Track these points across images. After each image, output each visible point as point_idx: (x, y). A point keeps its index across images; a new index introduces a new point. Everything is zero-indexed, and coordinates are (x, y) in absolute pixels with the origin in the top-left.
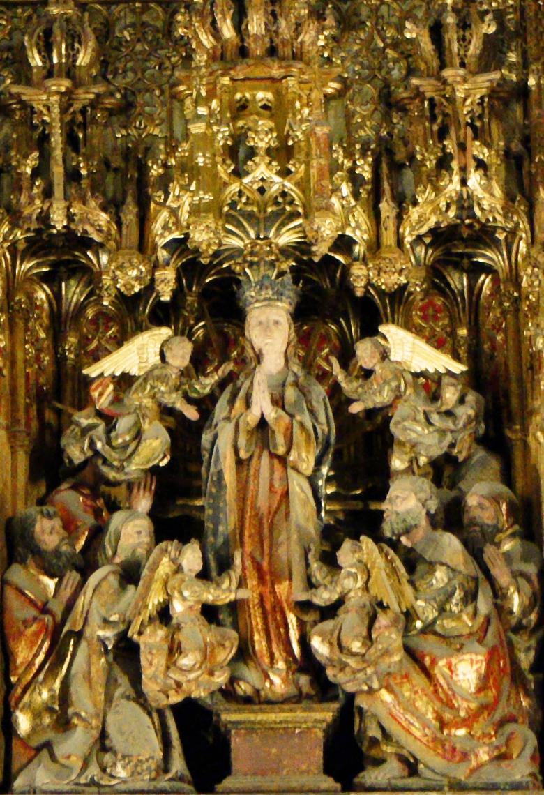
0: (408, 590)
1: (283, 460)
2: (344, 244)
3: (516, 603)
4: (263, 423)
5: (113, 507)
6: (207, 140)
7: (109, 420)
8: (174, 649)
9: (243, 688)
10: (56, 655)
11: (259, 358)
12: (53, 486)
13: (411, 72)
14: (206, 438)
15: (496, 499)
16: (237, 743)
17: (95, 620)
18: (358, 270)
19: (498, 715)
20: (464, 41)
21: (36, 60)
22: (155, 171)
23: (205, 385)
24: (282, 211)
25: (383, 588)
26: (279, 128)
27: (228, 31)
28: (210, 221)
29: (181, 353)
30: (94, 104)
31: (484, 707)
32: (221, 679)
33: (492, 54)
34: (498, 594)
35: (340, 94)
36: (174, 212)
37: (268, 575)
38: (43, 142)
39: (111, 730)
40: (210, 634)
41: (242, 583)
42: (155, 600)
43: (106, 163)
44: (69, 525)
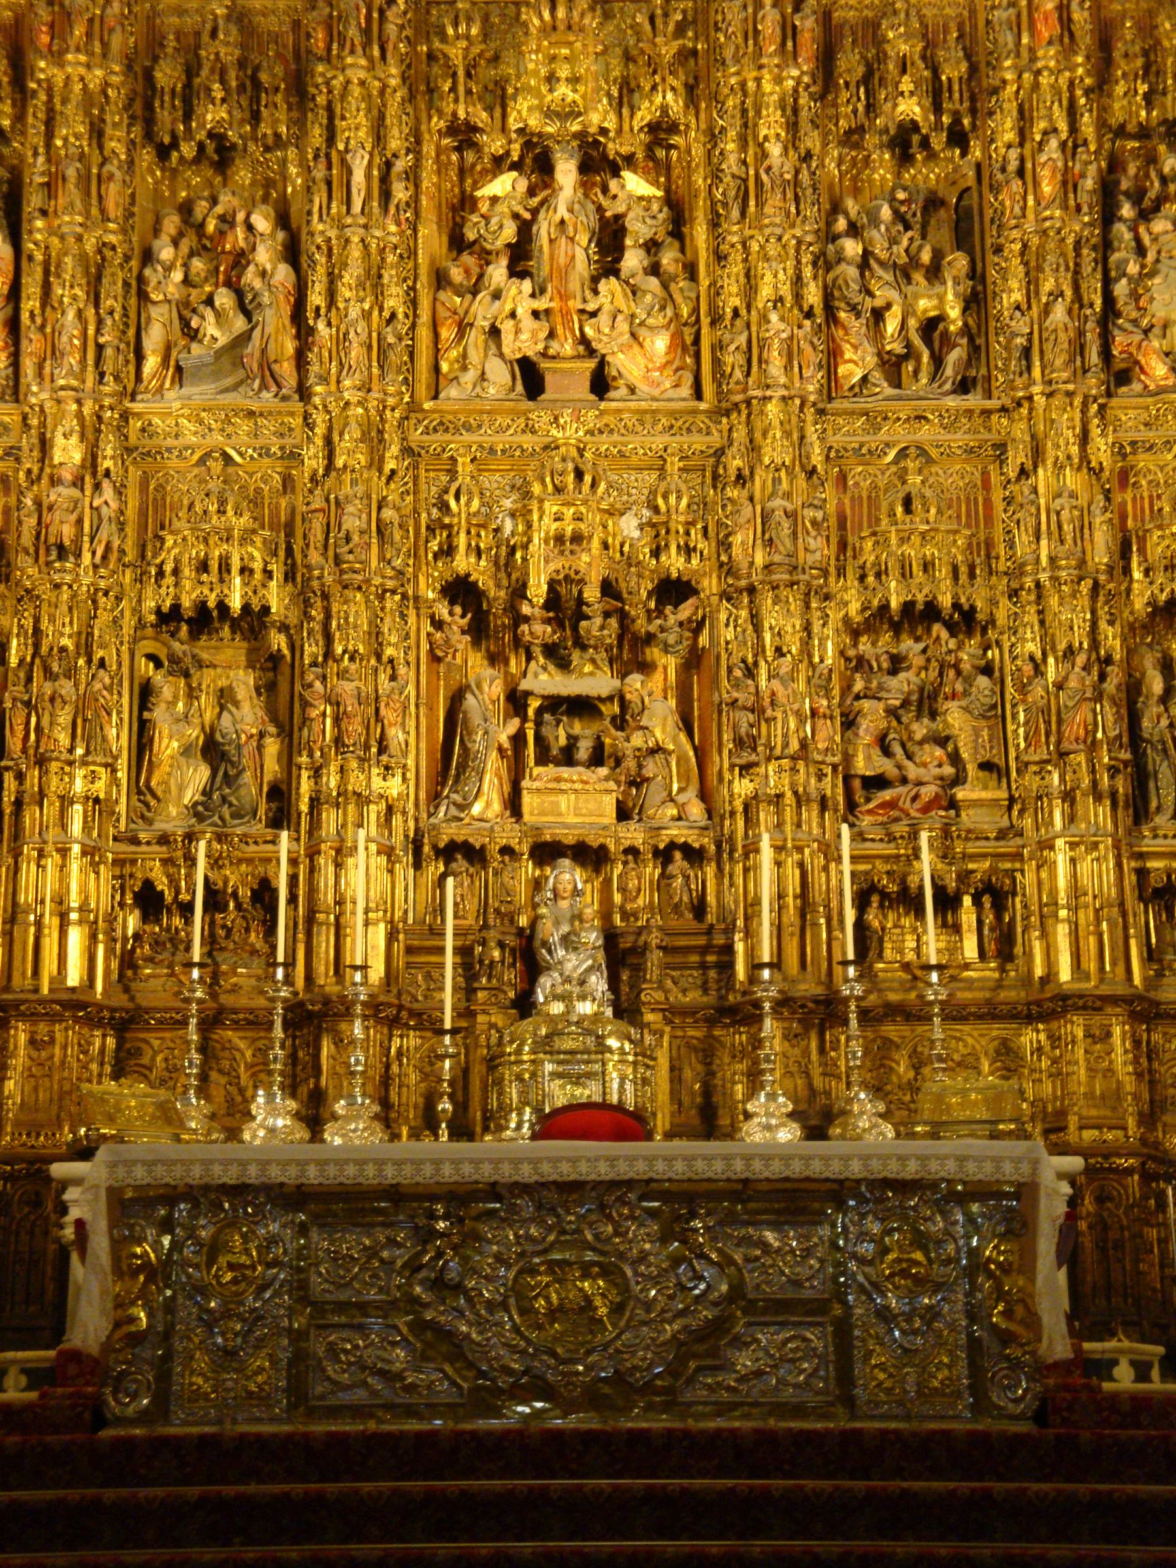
1: (572, 239)
2: (604, 131)
3: (685, 312)
4: (562, 222)
5: (488, 263)
6: (536, 72)
8: (518, 331)
9: (551, 352)
12: (460, 251)
13: (638, 40)
14: (535, 229)
15: (677, 261)
16: (548, 378)
17: (479, 317)
18: (610, 145)
19: (674, 366)
20: (666, 24)
21: (450, 31)
22: (510, 91)
23: (535, 201)
24: (573, 113)
25: (621, 302)
26: (572, 69)
27: (547, 15)
28: (537, 115)
29: (523, 185)
30: (480, 55)
31: (668, 363)
32: (540, 347)
33: (680, 30)
36: (519, 112)
37: (564, 297)
38: (454, 75)
39: (487, 370)
40: (536, 324)
41: (551, 300)
42: (508, 307)
43: (486, 88)
44: (467, 272)
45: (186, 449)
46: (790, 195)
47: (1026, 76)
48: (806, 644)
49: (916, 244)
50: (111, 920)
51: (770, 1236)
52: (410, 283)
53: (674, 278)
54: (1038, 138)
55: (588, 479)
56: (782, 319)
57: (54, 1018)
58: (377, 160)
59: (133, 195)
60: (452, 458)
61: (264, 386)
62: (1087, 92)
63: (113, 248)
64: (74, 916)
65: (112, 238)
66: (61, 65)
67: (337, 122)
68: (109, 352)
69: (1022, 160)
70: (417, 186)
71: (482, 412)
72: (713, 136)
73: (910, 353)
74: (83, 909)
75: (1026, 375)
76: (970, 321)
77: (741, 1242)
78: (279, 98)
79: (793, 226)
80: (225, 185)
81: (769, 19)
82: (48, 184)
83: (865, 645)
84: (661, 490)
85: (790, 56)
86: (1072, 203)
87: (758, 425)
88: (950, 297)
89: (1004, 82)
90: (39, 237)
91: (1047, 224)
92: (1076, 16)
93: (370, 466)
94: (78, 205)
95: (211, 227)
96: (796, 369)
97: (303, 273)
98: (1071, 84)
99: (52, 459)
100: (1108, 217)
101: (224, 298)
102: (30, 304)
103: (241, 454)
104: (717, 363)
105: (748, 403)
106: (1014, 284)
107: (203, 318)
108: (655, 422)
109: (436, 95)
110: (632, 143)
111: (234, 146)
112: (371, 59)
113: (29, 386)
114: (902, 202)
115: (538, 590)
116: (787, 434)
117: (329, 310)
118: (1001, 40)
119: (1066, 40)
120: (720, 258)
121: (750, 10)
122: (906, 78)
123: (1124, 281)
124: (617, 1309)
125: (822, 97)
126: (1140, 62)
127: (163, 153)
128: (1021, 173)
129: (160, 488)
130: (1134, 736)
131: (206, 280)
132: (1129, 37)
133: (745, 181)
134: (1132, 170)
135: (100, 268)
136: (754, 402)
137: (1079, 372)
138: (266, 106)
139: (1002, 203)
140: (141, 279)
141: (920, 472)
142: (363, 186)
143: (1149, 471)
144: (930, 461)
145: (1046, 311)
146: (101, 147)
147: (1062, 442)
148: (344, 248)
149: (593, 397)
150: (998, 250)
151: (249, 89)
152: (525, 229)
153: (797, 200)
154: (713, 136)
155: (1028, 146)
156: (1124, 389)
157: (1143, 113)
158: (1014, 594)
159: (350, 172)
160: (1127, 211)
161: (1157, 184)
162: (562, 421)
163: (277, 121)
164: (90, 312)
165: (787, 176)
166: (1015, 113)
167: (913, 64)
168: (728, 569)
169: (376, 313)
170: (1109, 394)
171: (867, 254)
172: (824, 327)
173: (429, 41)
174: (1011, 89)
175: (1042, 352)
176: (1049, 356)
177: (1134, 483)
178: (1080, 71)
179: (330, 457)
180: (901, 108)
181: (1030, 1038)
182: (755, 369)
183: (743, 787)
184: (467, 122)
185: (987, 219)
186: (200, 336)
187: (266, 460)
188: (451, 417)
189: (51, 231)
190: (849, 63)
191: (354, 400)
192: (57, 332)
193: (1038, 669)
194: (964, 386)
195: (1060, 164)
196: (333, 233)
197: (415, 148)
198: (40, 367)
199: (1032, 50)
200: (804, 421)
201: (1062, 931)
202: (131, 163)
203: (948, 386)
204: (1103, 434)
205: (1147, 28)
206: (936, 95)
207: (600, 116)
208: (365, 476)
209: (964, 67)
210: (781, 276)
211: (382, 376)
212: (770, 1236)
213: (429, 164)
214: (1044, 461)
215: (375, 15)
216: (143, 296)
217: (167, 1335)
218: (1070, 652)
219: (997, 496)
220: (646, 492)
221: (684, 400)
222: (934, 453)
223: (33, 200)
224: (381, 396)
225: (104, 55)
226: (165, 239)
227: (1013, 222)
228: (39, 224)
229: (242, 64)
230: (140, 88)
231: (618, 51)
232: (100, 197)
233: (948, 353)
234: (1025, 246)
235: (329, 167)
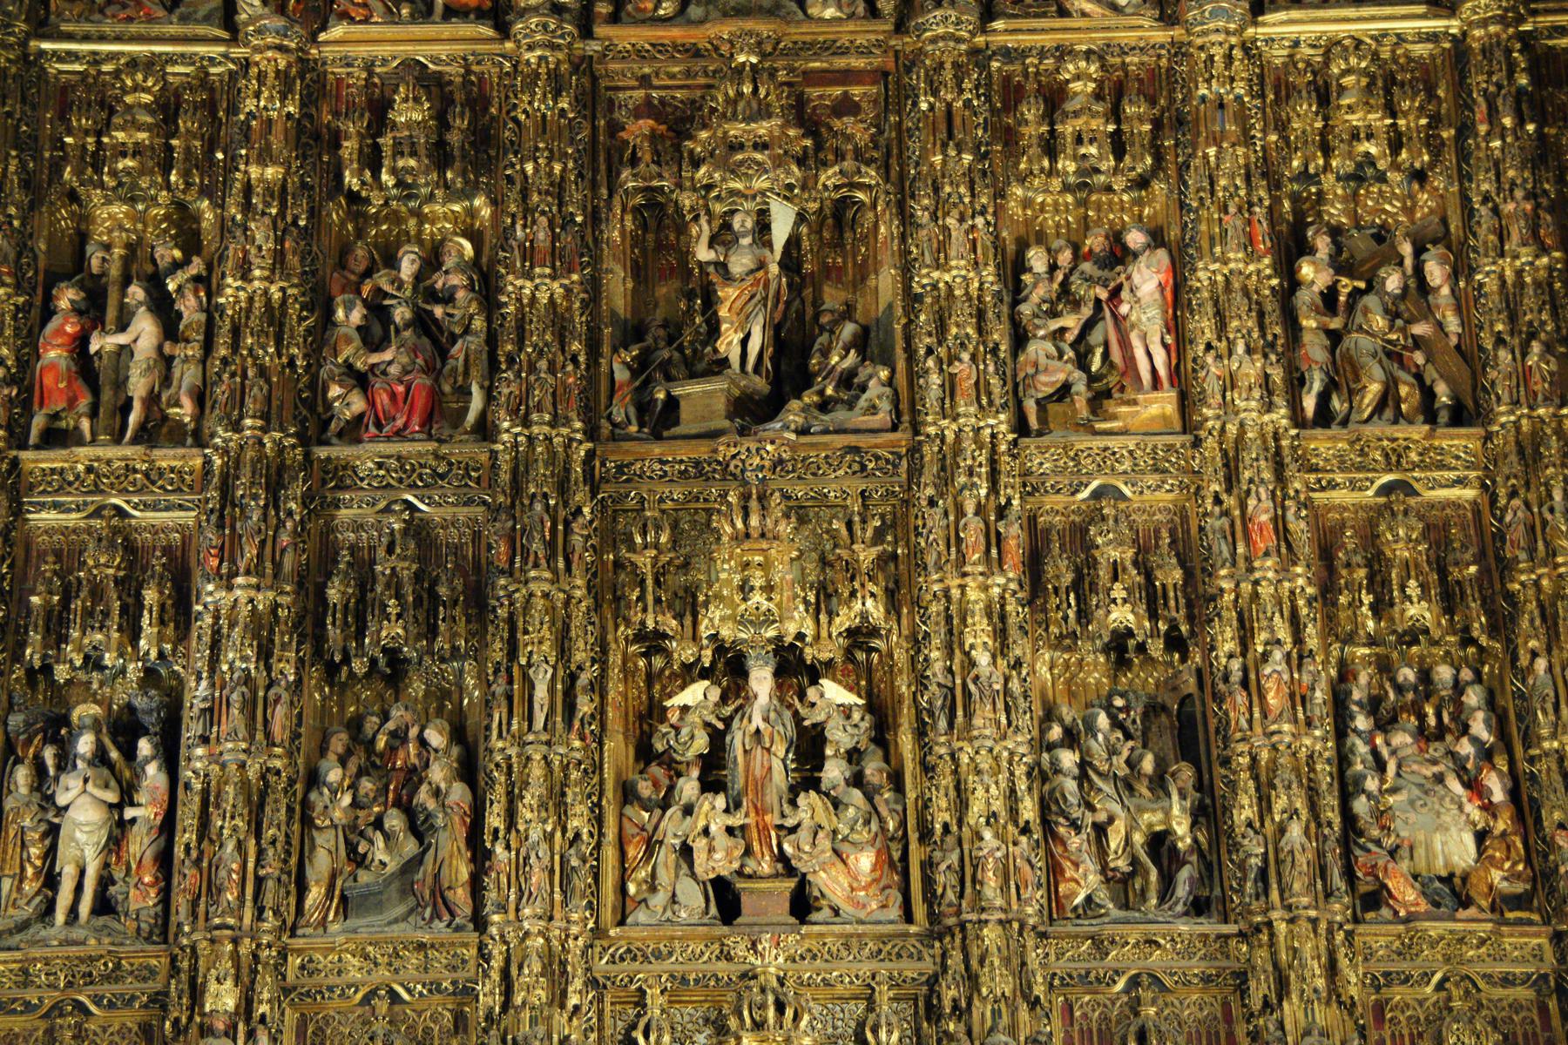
0: (834, 819)
1: (768, 750)
2: (800, 636)
3: (891, 825)
4: (758, 731)
5: (679, 775)
6: (729, 582)
7: (677, 729)
8: (711, 850)
9: (747, 870)
10: (649, 853)
11: (756, 697)
12: (647, 764)
13: (836, 546)
14: (728, 739)
15: (880, 771)
16: (744, 899)
17: (669, 834)
18: (808, 650)
19: (882, 884)
21: (639, 540)
22: (701, 598)
23: (727, 711)
25: (821, 817)
26: (766, 575)
27: (740, 525)
29: (715, 694)
30: (669, 563)
31: (875, 881)
32: (736, 865)
33: (879, 536)
34: (881, 820)
35: (799, 558)
36: (711, 620)
37: (760, 811)
39: (678, 892)
40: (730, 842)
41: (747, 815)
42: (701, 824)
44: (656, 784)
45: (349, 987)
46: (1000, 705)
47: (1243, 585)
49: (1137, 752)
52: (595, 799)
53: (878, 790)
54: (1260, 649)
55: (789, 1013)
56: (997, 835)
58: (561, 673)
59: (300, 715)
60: (640, 989)
61: (436, 915)
62: (1310, 601)
63: (278, 773)
65: (278, 764)
66: (230, 588)
67: (519, 635)
68: (270, 884)
69: (1245, 670)
70: (603, 697)
71: (672, 938)
72: (917, 642)
75: (1263, 898)
76: (1201, 838)
78: (457, 611)
79: (1004, 737)
80: (397, 700)
81: (972, 526)
82: (211, 710)
84: (870, 1023)
85: (995, 565)
86: (1301, 715)
87: (975, 952)
88: (1176, 811)
89: (1222, 590)
90: (199, 765)
91: (1275, 738)
92: (1291, 527)
93: (550, 1004)
94: (242, 733)
95: (381, 743)
96: (1013, 890)
97: (480, 792)
98: (1292, 592)
99: (202, 1006)
100: (1341, 730)
101: (395, 821)
102: (186, 836)
103: (409, 991)
104: (928, 882)
105: (962, 926)
106: (1245, 800)
107: (371, 842)
108: (863, 945)
109: (623, 603)
110: (828, 651)
111: (407, 661)
112: (555, 572)
113: (179, 925)
114: (1120, 709)
116: (1007, 961)
117: (508, 830)
118: (1215, 549)
119: (1284, 550)
120: (927, 769)
121: (952, 518)
122: (1118, 586)
123: (1363, 798)
125: (1030, 603)
126: (1361, 573)
127: (331, 670)
128: (1245, 683)
129: (319, 1031)
131: (375, 799)
132: (1350, 547)
133: (952, 690)
134: (1363, 678)
135: (263, 795)
136: (969, 926)
137: (1321, 896)
138: (444, 620)
139: (1226, 713)
140: (306, 804)
141: (1154, 1002)
142: (546, 702)
143: (1408, 1006)
144: (1163, 988)
145: (1282, 830)
146: (269, 668)
147: (1307, 974)
148: (525, 766)
149: (793, 920)
150: (1226, 762)
151: (425, 603)
152: (718, 739)
153: (1007, 710)
154: (917, 641)
155: (1250, 656)
156: (1370, 915)
157: (1371, 624)
159: (532, 687)
160: (1362, 722)
161: (1392, 695)
162: (760, 947)
163: (454, 635)
164: (251, 844)
165: (997, 687)
166: (1235, 623)
167: (1124, 569)
169: (558, 834)
170: (1356, 920)
171: (1084, 765)
172: (1042, 844)
173: (615, 548)
174: (1228, 598)
175: (1279, 874)
176: (1287, 879)
177: (1391, 1020)
178: (1300, 581)
179: (508, 992)
180: (1113, 616)
182: (968, 890)
184: (656, 631)
185: (1212, 729)
186: (367, 862)
187: (437, 997)
188: (639, 944)
189: (214, 758)
190: (1060, 571)
191: (535, 930)
192: (214, 866)
194: (1198, 907)
195: (1286, 677)
196: (513, 751)
197: (601, 658)
198: (194, 904)
199: (1248, 560)
200: (1024, 946)
202: (299, 681)
203: (1180, 908)
204: (1355, 967)
206: (1153, 600)
207: (798, 623)
208: (546, 1013)
209: (1177, 575)
210: (993, 790)
211: (565, 903)
213: (615, 673)
214: (1288, 994)
215: (560, 527)
216: (307, 822)
219: (1241, 1030)
220: (853, 1024)
221: (891, 922)
222: (1168, 982)
223: (191, 729)
224: (564, 924)
225: (275, 576)
226: (332, 757)
227: (1238, 735)
228: (200, 751)
229: (418, 577)
230: (310, 606)
231: (814, 555)
232: (266, 722)
233: (1178, 870)
234: (1254, 759)
235: (510, 682)
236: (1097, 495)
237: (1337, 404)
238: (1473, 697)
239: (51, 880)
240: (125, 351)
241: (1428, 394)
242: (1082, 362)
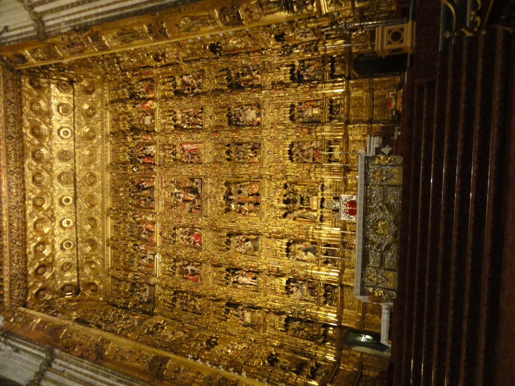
48: (294, 169)
50: (329, 268)
51: (374, 195)
57: (342, 278)
64: (328, 274)
73: (255, 152)
74: (327, 272)
77: (374, 199)
83: (294, 159)
101: (246, 243)
115: (284, 206)
124: (384, 220)
130: (309, 122)
158: (288, 139)
160: (238, 123)
168: (283, 178)
181: (351, 138)
183: (313, 178)
193: (298, 136)
201: (335, 134)
205: (216, 121)
212: (374, 195)
217: (384, 288)
218: (296, 132)
236: (210, 154)
237: (201, 124)
238: (236, 109)
239: (251, 285)
240: (191, 270)
241: (200, 113)
242: (195, 155)
